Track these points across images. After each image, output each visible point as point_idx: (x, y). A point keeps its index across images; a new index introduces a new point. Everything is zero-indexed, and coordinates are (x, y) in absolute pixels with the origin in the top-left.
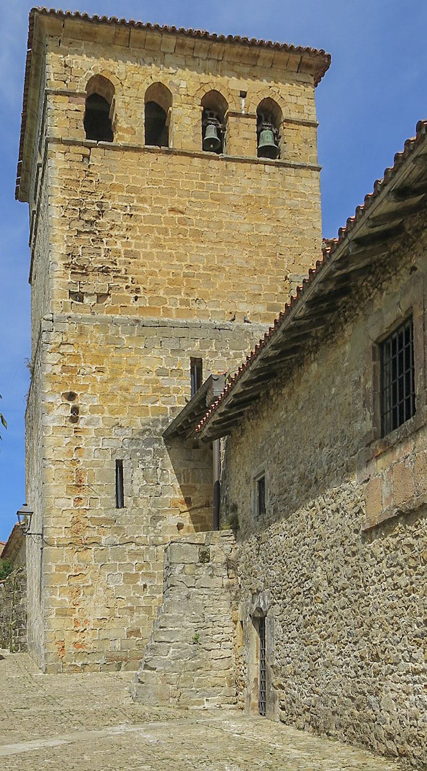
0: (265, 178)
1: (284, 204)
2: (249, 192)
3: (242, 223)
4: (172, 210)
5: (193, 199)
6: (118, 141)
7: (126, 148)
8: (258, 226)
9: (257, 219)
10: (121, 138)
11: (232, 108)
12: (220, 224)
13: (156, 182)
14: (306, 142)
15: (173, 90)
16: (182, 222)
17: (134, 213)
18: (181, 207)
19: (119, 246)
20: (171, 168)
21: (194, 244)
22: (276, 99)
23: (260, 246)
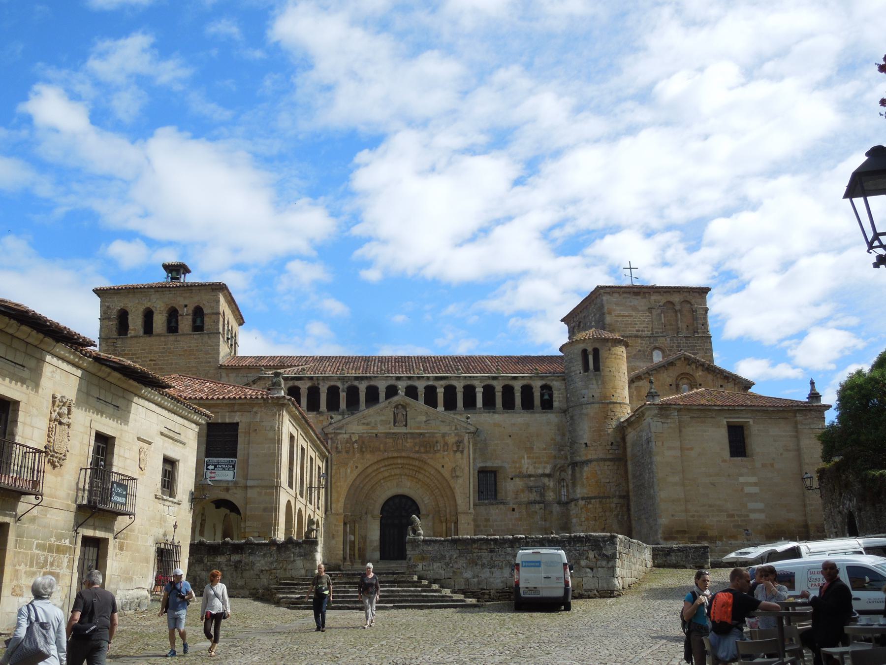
1: (201, 351)
4: (151, 360)
6: (129, 336)
7: (135, 337)
10: (131, 333)
11: (180, 312)
12: (172, 364)
13: (144, 350)
14: (214, 322)
15: (154, 309)
16: (155, 365)
18: (154, 359)
22: (201, 305)
23: (190, 371)
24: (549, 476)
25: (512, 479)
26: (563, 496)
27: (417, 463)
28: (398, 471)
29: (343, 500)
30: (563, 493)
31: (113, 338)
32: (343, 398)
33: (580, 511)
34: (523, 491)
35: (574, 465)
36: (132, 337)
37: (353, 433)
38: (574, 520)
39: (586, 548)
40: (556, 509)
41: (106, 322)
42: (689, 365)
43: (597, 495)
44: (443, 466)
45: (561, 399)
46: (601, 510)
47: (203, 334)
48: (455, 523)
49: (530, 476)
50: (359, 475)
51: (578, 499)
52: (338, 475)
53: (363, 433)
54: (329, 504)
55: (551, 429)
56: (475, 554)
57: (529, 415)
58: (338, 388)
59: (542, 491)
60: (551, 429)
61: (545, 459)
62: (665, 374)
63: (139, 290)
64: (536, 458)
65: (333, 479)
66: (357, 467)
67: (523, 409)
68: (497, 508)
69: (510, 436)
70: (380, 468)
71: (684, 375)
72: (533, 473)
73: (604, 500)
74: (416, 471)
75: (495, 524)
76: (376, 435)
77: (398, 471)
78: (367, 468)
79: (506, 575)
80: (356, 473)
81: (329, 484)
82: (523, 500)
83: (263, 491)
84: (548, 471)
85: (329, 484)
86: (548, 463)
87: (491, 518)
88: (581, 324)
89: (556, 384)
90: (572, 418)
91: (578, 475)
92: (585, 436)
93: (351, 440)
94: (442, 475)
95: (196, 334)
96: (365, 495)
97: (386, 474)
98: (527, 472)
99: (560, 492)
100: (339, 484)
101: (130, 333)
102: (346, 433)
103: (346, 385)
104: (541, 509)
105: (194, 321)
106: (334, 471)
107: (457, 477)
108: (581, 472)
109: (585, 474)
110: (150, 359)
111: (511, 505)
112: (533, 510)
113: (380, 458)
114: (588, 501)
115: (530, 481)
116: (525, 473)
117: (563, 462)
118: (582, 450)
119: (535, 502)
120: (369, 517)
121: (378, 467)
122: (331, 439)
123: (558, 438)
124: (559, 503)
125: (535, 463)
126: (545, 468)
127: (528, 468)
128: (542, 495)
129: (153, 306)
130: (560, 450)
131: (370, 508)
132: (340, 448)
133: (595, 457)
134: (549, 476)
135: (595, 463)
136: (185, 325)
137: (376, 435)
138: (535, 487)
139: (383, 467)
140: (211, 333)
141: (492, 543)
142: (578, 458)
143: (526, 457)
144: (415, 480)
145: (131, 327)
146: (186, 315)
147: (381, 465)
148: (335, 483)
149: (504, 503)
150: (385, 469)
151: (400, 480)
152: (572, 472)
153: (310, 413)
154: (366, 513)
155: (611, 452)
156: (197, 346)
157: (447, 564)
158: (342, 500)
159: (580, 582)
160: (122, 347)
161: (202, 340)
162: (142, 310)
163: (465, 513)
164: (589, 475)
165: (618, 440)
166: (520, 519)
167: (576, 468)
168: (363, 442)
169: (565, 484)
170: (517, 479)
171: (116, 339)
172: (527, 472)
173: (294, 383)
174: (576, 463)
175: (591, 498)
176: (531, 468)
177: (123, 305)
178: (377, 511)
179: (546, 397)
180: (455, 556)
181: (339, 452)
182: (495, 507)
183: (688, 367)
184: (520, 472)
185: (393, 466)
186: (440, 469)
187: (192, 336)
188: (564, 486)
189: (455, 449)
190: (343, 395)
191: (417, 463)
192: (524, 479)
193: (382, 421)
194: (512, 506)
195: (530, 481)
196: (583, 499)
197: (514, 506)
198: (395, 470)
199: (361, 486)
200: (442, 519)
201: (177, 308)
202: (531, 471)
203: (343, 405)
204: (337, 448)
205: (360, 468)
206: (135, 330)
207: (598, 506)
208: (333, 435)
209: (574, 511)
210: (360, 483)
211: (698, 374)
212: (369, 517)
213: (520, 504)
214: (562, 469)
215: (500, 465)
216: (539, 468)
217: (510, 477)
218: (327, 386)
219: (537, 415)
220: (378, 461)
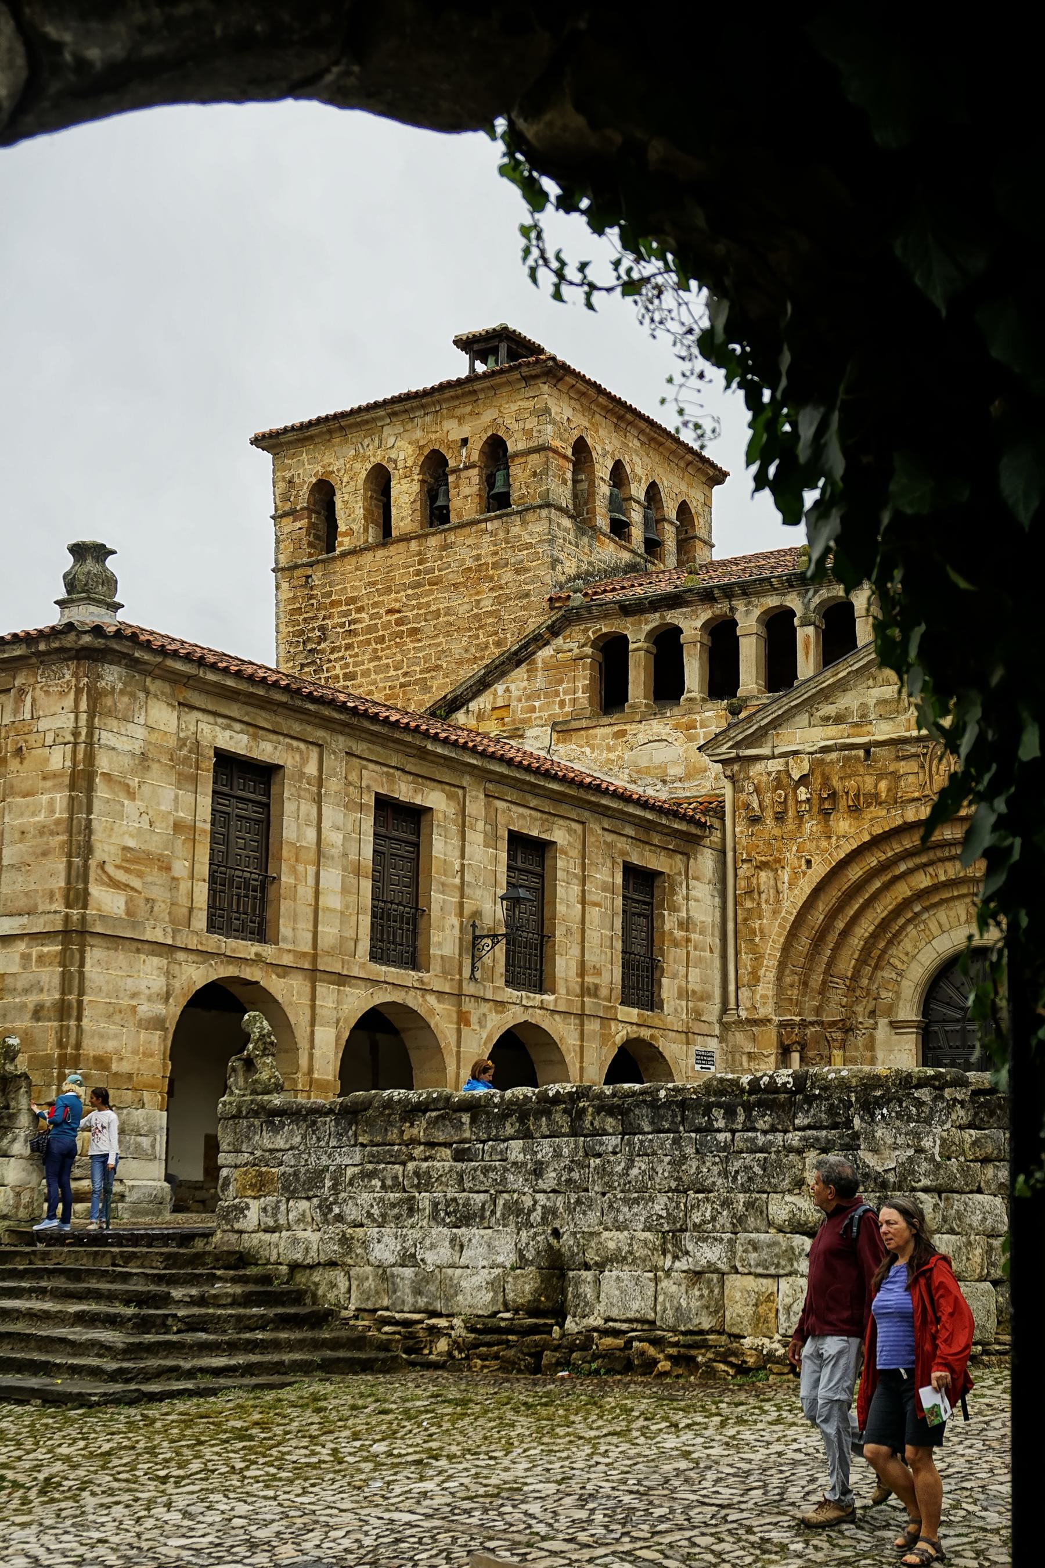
0: (487, 538)
1: (506, 565)
2: (469, 563)
3: (461, 604)
4: (390, 611)
5: (410, 592)
6: (338, 550)
7: (354, 552)
8: (478, 601)
9: (478, 593)
10: (344, 543)
11: (452, 463)
12: (437, 614)
15: (390, 467)
16: (399, 622)
17: (352, 627)
18: (397, 605)
19: (338, 671)
20: (389, 561)
21: (411, 646)
23: (480, 627)
29: (771, 975)
31: (304, 565)
36: (344, 555)
37: (795, 753)
39: (794, 1138)
41: (289, 525)
47: (507, 515)
52: (756, 896)
53: (825, 750)
54: (732, 988)
56: (411, 1166)
58: (792, 613)
63: (352, 420)
65: (739, 912)
66: (809, 862)
76: (867, 752)
79: (500, 1259)
80: (806, 886)
81: (730, 926)
83: (35, 951)
85: (730, 926)
93: (790, 776)
95: (491, 519)
97: (923, 881)
100: (756, 925)
101: (341, 544)
102: (774, 757)
103: (817, 600)
105: (489, 481)
106: (742, 883)
110: (388, 607)
120: (882, 1032)
122: (732, 779)
129: (390, 460)
131: (884, 994)
132: (755, 805)
136: (466, 497)
137: (867, 752)
140: (527, 510)
141: (466, 1118)
145: (342, 527)
146: (466, 468)
148: (746, 920)
150: (910, 864)
153: (709, 705)
154: (872, 1013)
156: (496, 553)
157: (325, 1208)
158: (768, 974)
159: (770, 1298)
160: (324, 585)
161: (508, 532)
162: (364, 474)
168: (826, 780)
171: (311, 565)
173: (662, 617)
177: (321, 470)
178: (908, 1011)
180: (350, 1171)
181: (755, 820)
187: (483, 525)
190: (806, 636)
193: (882, 702)
199: (840, 925)
201: (444, 451)
203: (806, 665)
204: (747, 806)
205: (820, 870)
206: (350, 532)
208: (736, 767)
210: (832, 915)
212: (882, 1032)
218: (757, 612)
220: (876, 842)
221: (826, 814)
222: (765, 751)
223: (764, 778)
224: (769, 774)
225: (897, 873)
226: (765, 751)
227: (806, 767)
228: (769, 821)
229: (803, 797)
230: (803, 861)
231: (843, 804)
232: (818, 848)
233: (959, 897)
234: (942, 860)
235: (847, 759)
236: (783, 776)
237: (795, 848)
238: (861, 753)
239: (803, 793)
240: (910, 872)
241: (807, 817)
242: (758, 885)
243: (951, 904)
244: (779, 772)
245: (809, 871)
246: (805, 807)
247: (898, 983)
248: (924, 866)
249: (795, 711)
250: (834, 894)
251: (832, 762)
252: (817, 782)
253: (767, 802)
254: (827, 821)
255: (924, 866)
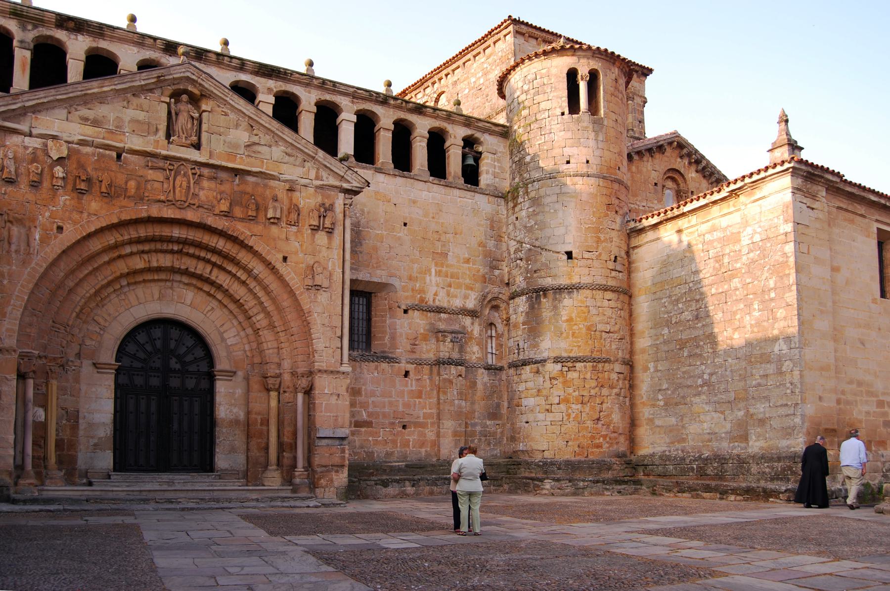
24: (473, 314)
25: (406, 312)
26: (490, 356)
27: (221, 244)
28: (166, 261)
30: (489, 350)
32: (24, 65)
33: (548, 384)
34: (425, 338)
35: (537, 293)
38: (529, 402)
40: (483, 378)
42: (681, 157)
43: (589, 354)
44: (285, 259)
45: (497, 170)
46: (594, 383)
48: (305, 393)
49: (439, 310)
50: (64, 252)
51: (545, 361)
53: (82, 143)
55: (479, 225)
57: (442, 189)
59: (460, 338)
60: (479, 225)
61: (468, 281)
62: (649, 163)
64: (452, 277)
66: (60, 229)
67: (431, 176)
68: (376, 368)
69: (405, 224)
70: (123, 244)
71: (673, 175)
72: (445, 305)
73: (600, 365)
74: (214, 265)
75: (371, 400)
77: (166, 261)
78: (90, 236)
82: (424, 356)
84: (471, 304)
86: (472, 289)
87: (364, 388)
88: (443, 96)
89: (489, 143)
90: (536, 202)
91: (546, 313)
92: (569, 239)
94: (280, 278)
96: (77, 310)
97: (138, 263)
98: (434, 300)
99: (486, 348)
102: (30, 135)
104: (460, 375)
107: (318, 287)
108: (555, 308)
109: (563, 313)
111: (402, 365)
112: (446, 376)
113: (125, 217)
114: (570, 364)
115: (440, 319)
116: (431, 303)
117: (496, 290)
118: (560, 264)
119: (450, 362)
121: (121, 239)
123: (491, 244)
124: (488, 368)
125: (450, 286)
126: (466, 297)
127: (436, 294)
128: (461, 350)
130: (493, 268)
132: (13, 170)
133: (586, 280)
134: (473, 314)
135: (588, 292)
138: (452, 333)
139: (131, 242)
142: (549, 279)
143: (433, 271)
144: (206, 288)
147: (126, 237)
149: (391, 360)
150: (135, 248)
151: (169, 284)
152: (532, 307)
155: (614, 274)
163: (332, 372)
164: (573, 315)
165: (623, 254)
166: (419, 395)
167: (543, 300)
169: (494, 334)
170: (417, 313)
172: (434, 300)
174: (545, 290)
175: (577, 360)
176: (442, 294)
179: (470, 161)
182: (373, 365)
183: (679, 160)
184: (422, 300)
185: (159, 246)
186: (279, 265)
188: (491, 337)
189: (316, 223)
190: (22, 58)
191: (221, 244)
192: (429, 314)
194: (404, 366)
195: (440, 319)
196: (557, 360)
197: (410, 367)
198: (161, 256)
200: (271, 381)
202: (442, 300)
203: (21, 79)
205: (71, 234)
207: (588, 376)
209: (530, 385)
211: (690, 175)
213: (419, 363)
214: (494, 303)
215: (384, 281)
216: (456, 296)
217: (404, 307)
219: (457, 192)
221: (82, 193)
222: (24, 127)
223: (21, 150)
224: (26, 148)
225: (123, 253)
226: (24, 127)
227: (65, 153)
228: (24, 187)
229: (61, 175)
230: (55, 226)
231: (96, 189)
232: (70, 219)
233: (154, 281)
234: (157, 251)
235: (101, 156)
236: (40, 153)
237: (47, 214)
238: (114, 154)
239: (59, 171)
240: (132, 254)
241: (61, 191)
242: (9, 236)
243: (148, 285)
244: (36, 149)
245: (61, 236)
246: (60, 183)
247: (101, 335)
248: (143, 252)
249: (56, 104)
250: (76, 257)
251: (87, 154)
252: (72, 165)
253: (22, 170)
254: (79, 199)
255: (143, 252)
